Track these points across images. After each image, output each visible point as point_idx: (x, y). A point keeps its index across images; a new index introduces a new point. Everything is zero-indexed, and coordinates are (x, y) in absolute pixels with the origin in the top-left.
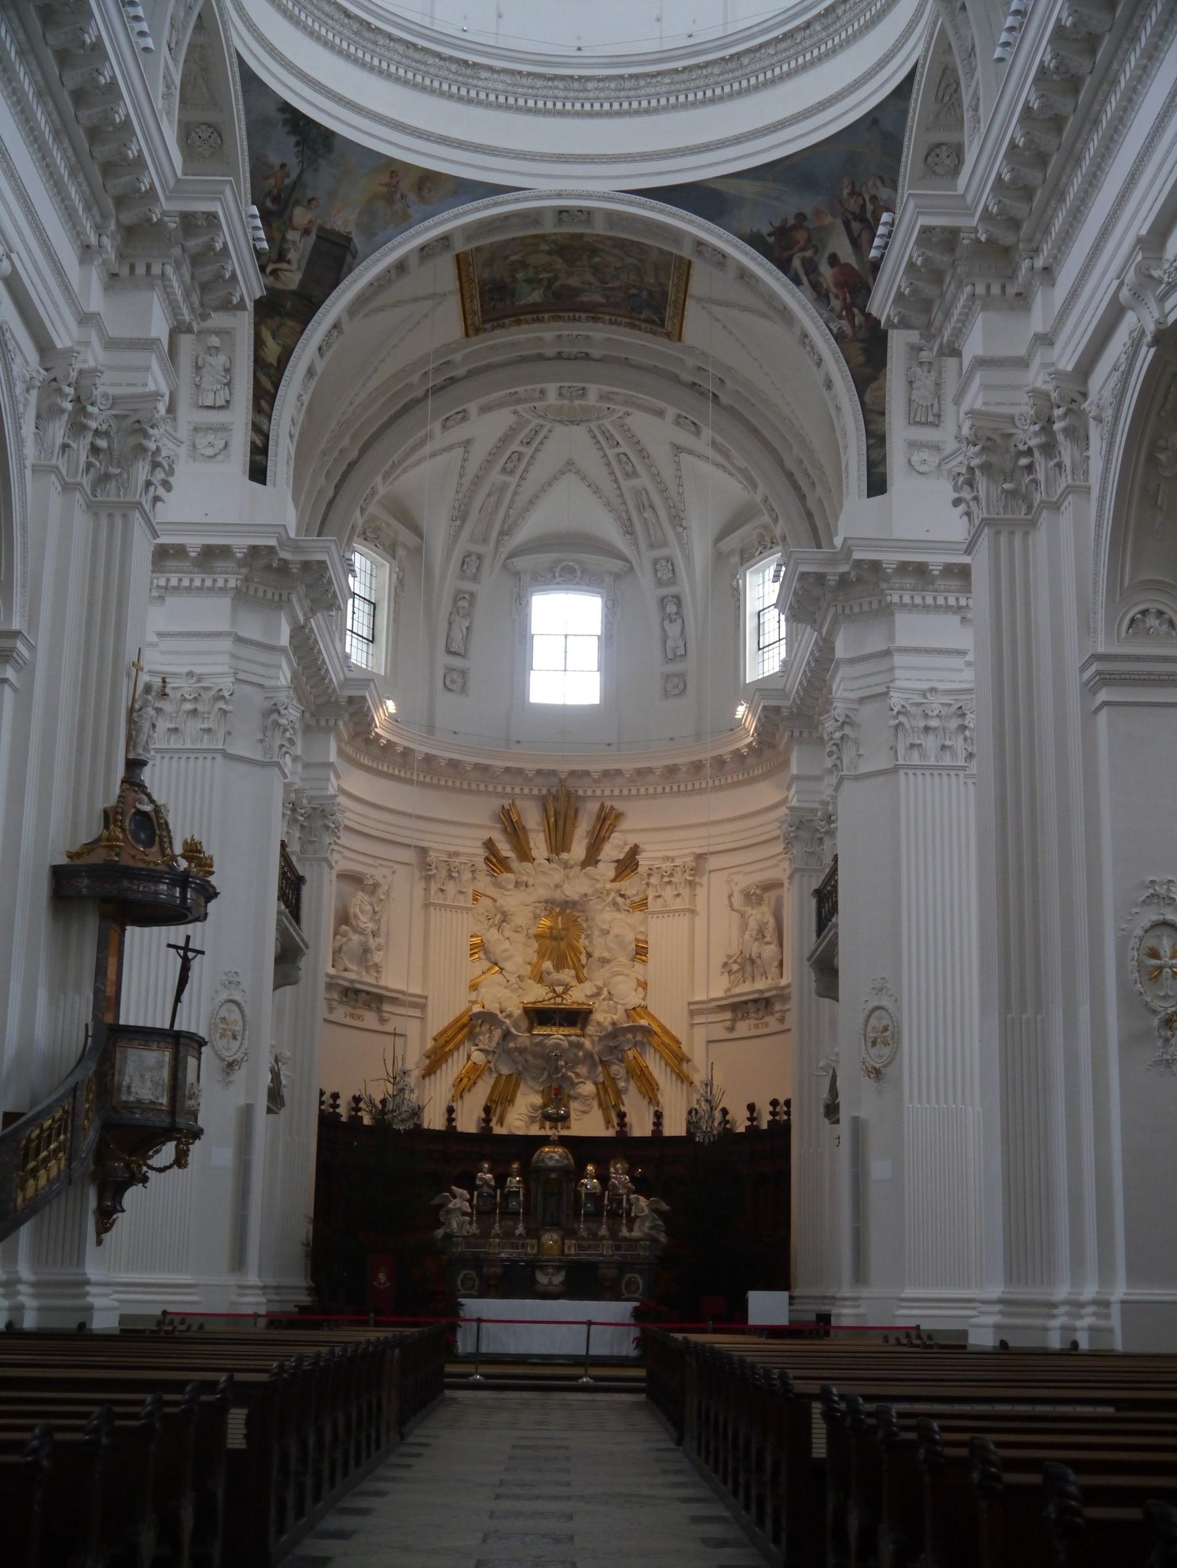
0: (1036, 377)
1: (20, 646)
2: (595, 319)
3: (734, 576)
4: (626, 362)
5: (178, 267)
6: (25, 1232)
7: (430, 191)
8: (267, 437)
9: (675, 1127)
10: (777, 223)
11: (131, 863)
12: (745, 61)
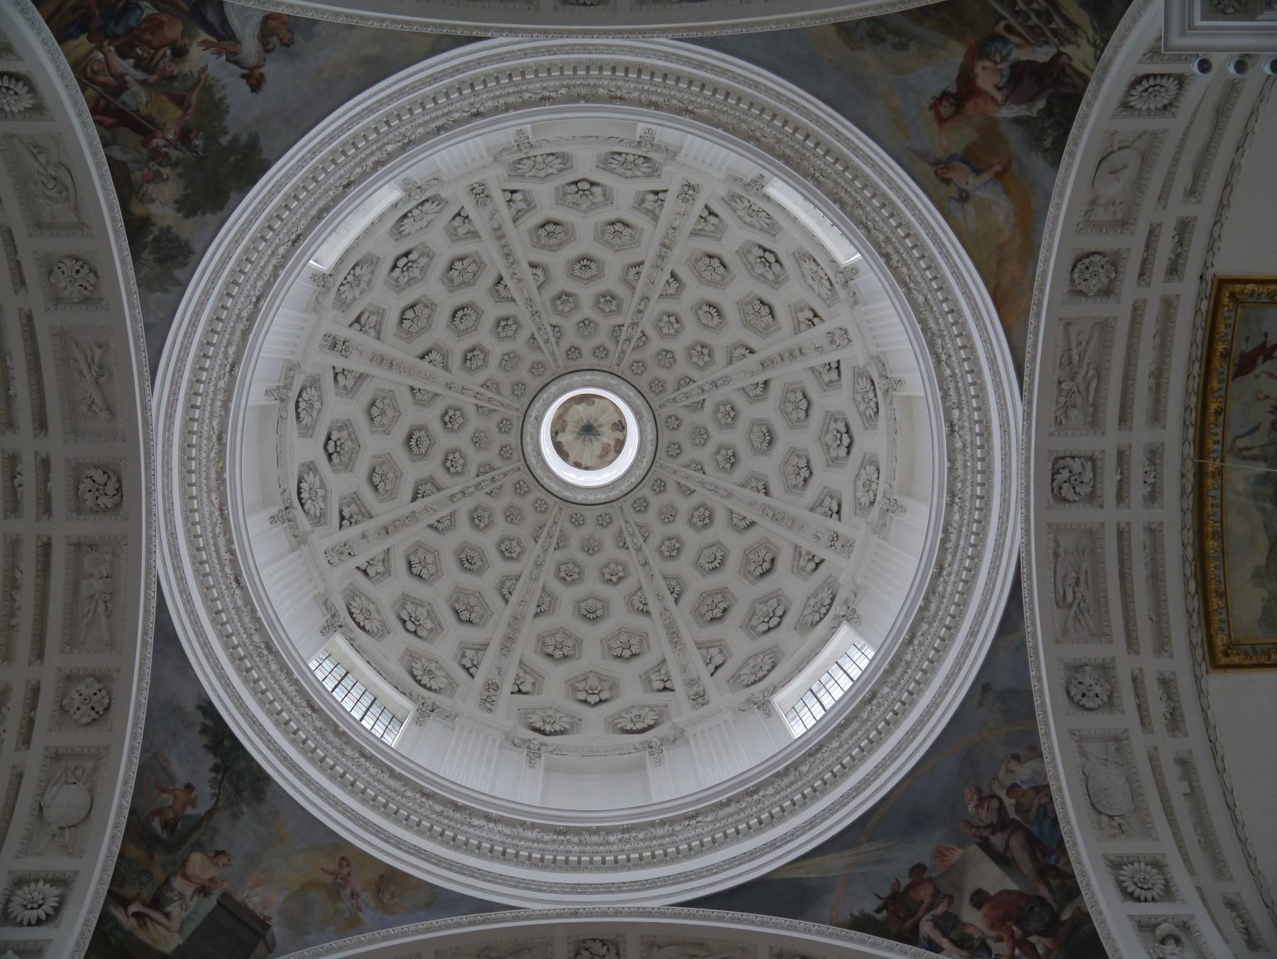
7: (393, 895)
10: (886, 892)
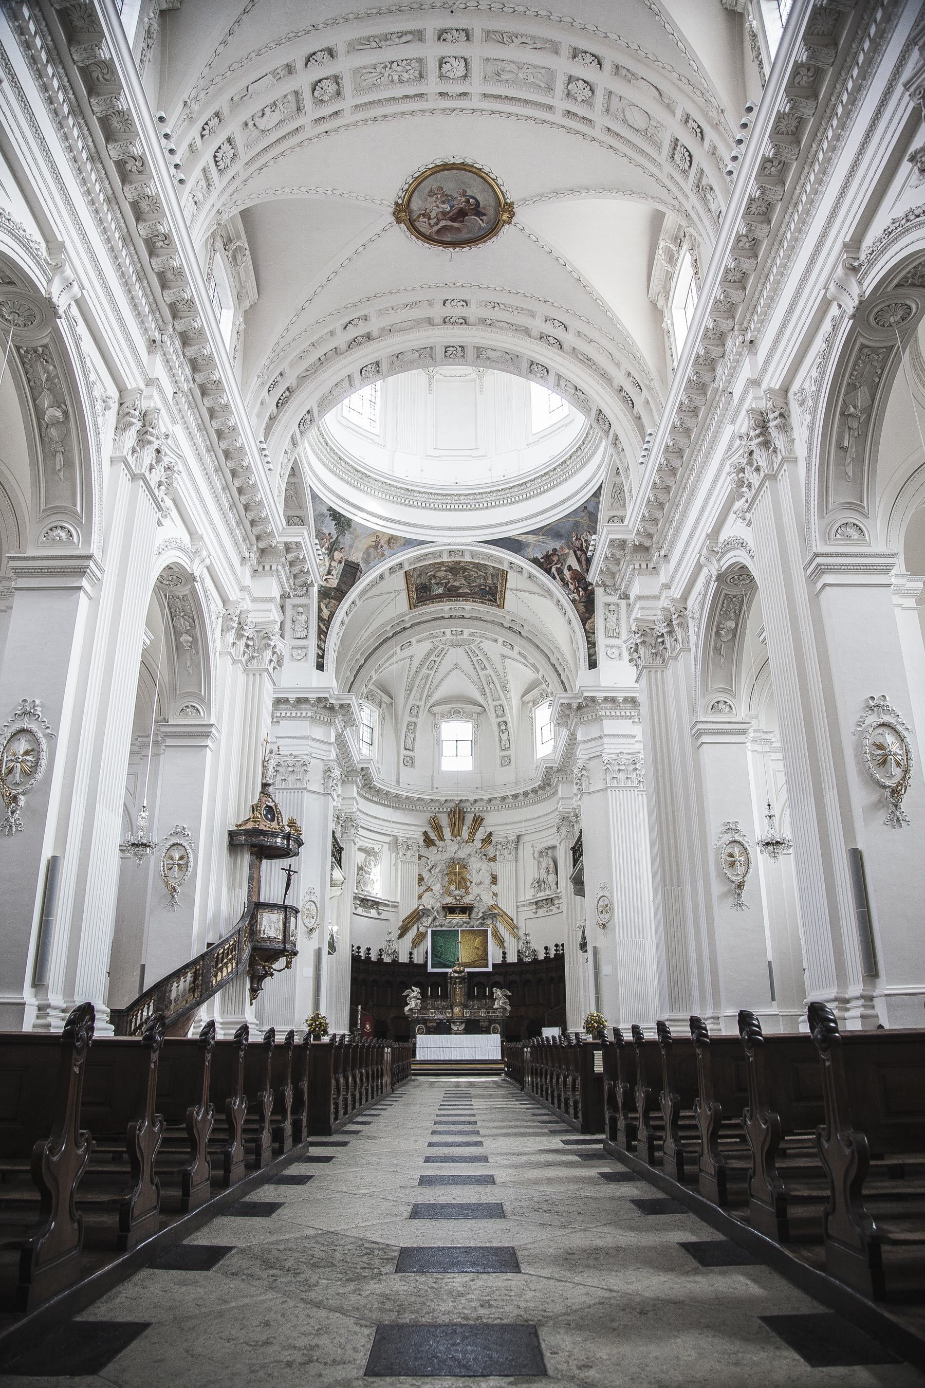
0: (664, 602)
1: (214, 730)
2: (466, 600)
3: (530, 712)
4: (480, 619)
5: (284, 567)
6: (217, 996)
8: (324, 651)
9: (512, 958)
11: (264, 829)
12: (528, 485)
